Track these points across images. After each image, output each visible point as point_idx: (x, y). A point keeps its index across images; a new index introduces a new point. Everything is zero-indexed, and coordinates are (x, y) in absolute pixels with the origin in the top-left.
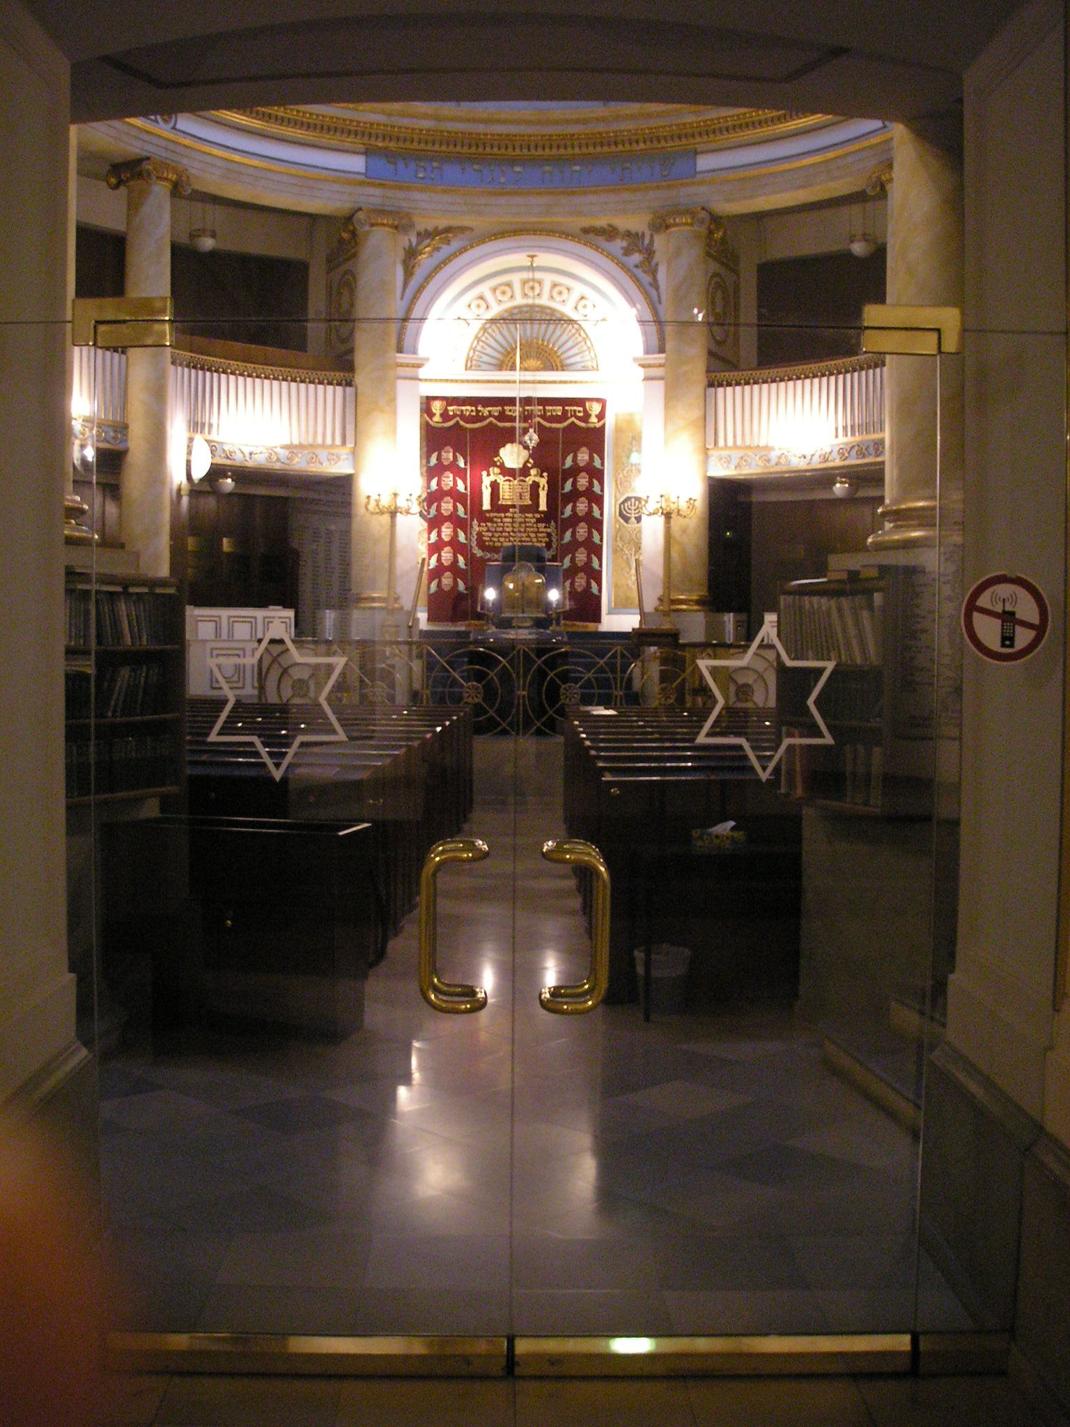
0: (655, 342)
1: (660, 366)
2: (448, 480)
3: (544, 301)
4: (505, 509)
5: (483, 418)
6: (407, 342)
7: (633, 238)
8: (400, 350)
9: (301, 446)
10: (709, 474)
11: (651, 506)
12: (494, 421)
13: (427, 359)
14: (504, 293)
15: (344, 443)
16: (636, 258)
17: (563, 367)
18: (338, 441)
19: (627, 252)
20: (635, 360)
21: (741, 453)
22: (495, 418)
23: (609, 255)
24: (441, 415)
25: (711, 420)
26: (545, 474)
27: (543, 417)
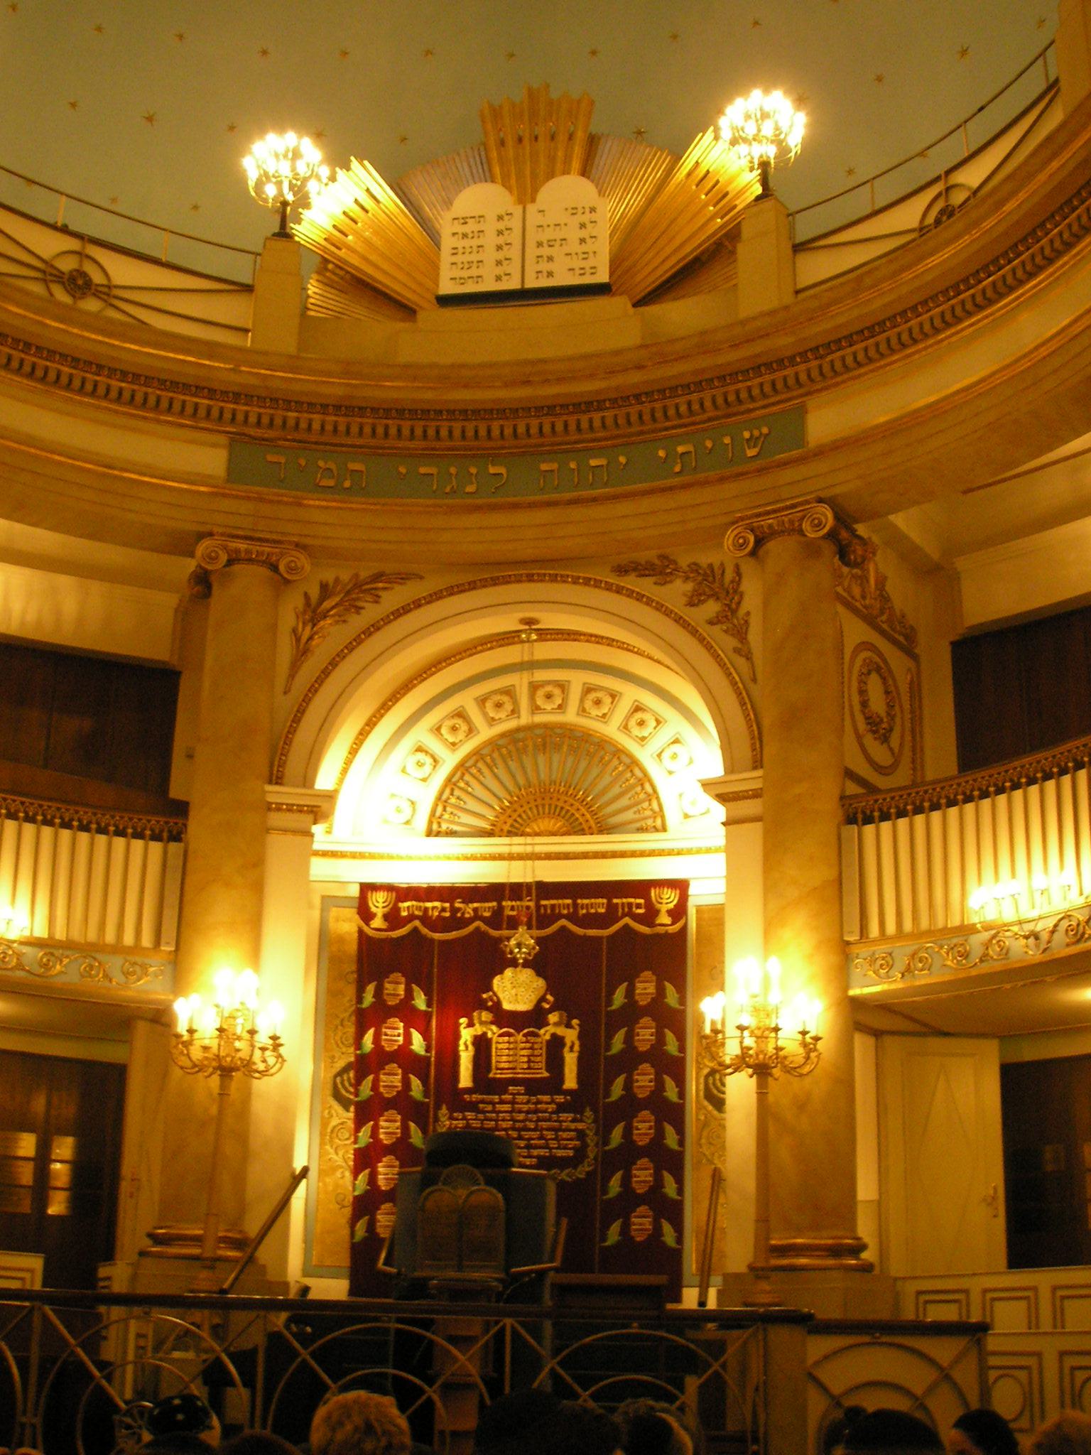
0: (744, 751)
1: (756, 794)
2: (395, 1032)
3: (570, 716)
4: (499, 1086)
5: (464, 923)
6: (294, 765)
8: (276, 778)
9: (69, 945)
10: (853, 992)
11: (731, 1050)
12: (483, 927)
13: (331, 797)
14: (499, 705)
16: (711, 608)
17: (604, 829)
18: (147, 941)
19: (694, 601)
20: (707, 785)
21: (910, 947)
22: (484, 919)
25: (851, 887)
26: (575, 1022)
27: (572, 917)
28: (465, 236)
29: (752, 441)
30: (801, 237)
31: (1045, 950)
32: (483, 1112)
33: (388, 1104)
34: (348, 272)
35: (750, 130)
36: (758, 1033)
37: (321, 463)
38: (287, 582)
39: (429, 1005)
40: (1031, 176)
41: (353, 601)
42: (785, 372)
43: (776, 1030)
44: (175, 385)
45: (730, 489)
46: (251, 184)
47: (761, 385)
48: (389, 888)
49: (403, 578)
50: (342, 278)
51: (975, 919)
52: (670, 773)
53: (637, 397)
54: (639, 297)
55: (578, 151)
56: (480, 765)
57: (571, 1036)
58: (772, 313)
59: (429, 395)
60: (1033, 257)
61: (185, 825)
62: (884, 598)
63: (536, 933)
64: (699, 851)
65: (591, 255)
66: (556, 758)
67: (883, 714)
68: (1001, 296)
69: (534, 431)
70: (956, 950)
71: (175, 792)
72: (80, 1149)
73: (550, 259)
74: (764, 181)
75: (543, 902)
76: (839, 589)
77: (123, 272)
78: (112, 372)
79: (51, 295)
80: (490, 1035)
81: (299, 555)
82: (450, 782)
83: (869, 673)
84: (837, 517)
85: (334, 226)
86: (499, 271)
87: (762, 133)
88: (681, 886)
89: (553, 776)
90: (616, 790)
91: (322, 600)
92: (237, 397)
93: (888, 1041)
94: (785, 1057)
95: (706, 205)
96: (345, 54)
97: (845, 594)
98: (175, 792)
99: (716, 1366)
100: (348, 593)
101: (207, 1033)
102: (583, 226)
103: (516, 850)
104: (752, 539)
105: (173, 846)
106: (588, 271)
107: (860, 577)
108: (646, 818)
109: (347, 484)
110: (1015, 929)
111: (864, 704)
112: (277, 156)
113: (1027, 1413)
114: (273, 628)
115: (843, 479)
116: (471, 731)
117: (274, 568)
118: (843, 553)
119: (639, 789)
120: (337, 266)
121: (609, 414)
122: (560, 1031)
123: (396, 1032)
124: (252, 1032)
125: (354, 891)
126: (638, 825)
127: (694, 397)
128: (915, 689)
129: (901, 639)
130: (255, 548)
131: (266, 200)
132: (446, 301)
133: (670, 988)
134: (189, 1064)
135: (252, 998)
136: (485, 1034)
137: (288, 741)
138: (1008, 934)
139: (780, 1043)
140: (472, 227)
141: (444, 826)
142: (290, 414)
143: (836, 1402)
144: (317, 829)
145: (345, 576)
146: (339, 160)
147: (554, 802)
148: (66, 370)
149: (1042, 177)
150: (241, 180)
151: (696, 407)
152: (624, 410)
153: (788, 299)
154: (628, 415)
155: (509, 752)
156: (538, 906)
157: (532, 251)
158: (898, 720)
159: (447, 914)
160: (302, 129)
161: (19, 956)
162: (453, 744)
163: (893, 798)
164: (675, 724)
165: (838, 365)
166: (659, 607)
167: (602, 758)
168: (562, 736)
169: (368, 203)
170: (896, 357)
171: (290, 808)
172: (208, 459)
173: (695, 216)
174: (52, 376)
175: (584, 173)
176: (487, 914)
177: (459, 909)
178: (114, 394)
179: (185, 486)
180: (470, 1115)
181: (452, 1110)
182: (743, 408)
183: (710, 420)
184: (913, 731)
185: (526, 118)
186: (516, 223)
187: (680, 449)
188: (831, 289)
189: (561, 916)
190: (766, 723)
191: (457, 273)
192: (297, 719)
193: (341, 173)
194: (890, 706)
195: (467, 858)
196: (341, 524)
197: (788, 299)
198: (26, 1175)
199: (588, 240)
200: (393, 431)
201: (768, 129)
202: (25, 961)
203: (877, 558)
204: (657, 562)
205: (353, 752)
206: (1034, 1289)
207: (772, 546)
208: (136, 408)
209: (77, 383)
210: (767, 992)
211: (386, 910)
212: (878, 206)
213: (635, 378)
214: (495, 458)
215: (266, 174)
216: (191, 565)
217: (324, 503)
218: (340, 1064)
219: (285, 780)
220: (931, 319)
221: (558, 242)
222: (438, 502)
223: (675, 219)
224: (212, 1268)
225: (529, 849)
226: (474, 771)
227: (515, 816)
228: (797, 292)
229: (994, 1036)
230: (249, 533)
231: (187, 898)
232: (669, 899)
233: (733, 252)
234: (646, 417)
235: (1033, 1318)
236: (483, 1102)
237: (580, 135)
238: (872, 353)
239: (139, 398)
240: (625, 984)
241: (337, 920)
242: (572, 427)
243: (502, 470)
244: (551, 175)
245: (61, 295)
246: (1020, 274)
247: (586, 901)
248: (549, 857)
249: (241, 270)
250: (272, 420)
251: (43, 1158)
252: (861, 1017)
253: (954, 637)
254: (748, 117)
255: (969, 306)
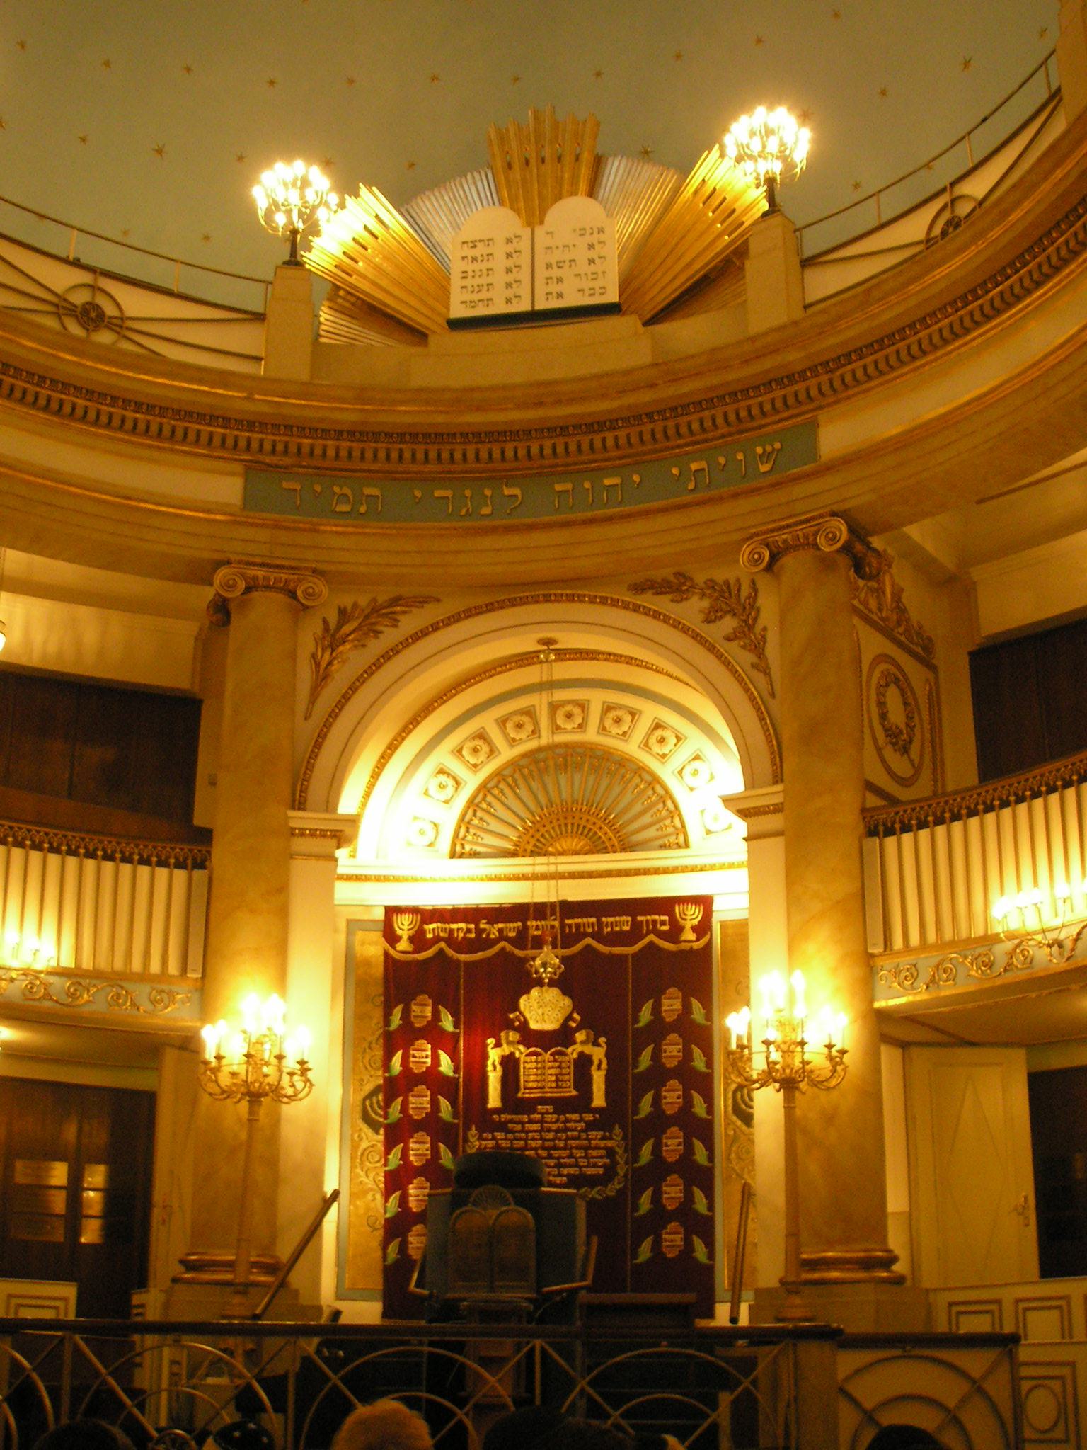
0: (764, 765)
1: (777, 809)
2: (423, 1054)
3: (591, 735)
4: (528, 1106)
5: (489, 943)
9: (97, 975)
10: (878, 1004)
11: (758, 1065)
12: (509, 947)
13: (353, 821)
14: (519, 726)
15: (184, 969)
16: (729, 624)
17: (627, 847)
18: (173, 969)
19: (711, 617)
20: (728, 801)
24: (411, 939)
26: (602, 1040)
27: (598, 936)
28: (474, 259)
29: (765, 456)
30: (807, 253)
31: (1069, 958)
32: (512, 1132)
33: (418, 1126)
34: (358, 298)
35: (756, 146)
36: (784, 1047)
37: (336, 489)
38: (306, 608)
39: (456, 1026)
40: (1034, 186)
41: (374, 623)
42: (796, 387)
43: (802, 1044)
44: (189, 415)
45: (744, 505)
46: (261, 213)
47: (773, 401)
48: (414, 910)
49: (422, 601)
50: (353, 304)
51: (998, 929)
52: (692, 789)
53: (650, 415)
54: (649, 316)
55: (585, 172)
56: (502, 786)
57: (598, 1054)
58: (782, 328)
59: (440, 419)
60: (1040, 265)
61: (209, 853)
62: (900, 609)
63: (561, 952)
64: (722, 867)
65: (601, 275)
66: (577, 778)
67: (903, 726)
68: (1010, 306)
69: (548, 451)
70: (980, 960)
71: (199, 820)
72: (112, 1177)
73: (560, 280)
74: (771, 197)
75: (568, 921)
76: (855, 602)
77: (134, 303)
78: (126, 403)
79: (65, 328)
80: (517, 1055)
81: (315, 580)
82: (472, 803)
83: (887, 685)
84: (851, 530)
85: (344, 253)
86: (510, 293)
87: (767, 150)
88: (704, 902)
89: (575, 795)
90: (638, 808)
91: (340, 625)
92: (251, 426)
93: (915, 1052)
94: (812, 1071)
95: (714, 222)
96: (351, 81)
97: (861, 607)
98: (199, 820)
99: (746, 1383)
100: (367, 617)
101: (235, 1059)
102: (591, 246)
103: (540, 869)
104: (767, 554)
105: (198, 874)
106: (598, 291)
107: (877, 590)
108: (670, 835)
109: (363, 509)
110: (1039, 937)
111: (883, 716)
112: (285, 185)
113: (1061, 1426)
114: (293, 656)
115: (857, 492)
116: (492, 752)
117: (293, 594)
118: (858, 566)
119: (661, 806)
120: (349, 293)
121: (622, 434)
122: (588, 1049)
123: (424, 1054)
124: (280, 1058)
125: (380, 914)
126: (661, 842)
127: (707, 414)
128: (934, 702)
129: (919, 650)
130: (273, 575)
131: (276, 229)
132: (457, 325)
133: (696, 1004)
134: (217, 1090)
135: (280, 1023)
136: (512, 1054)
137: (310, 767)
138: (1031, 943)
139: (806, 1057)
140: (480, 250)
141: (468, 848)
142: (305, 441)
143: (869, 1417)
144: (341, 854)
145: (363, 601)
146: (347, 186)
147: (576, 821)
148: (81, 402)
149: (1046, 186)
150: (251, 208)
151: (708, 424)
152: (638, 429)
153: (798, 314)
154: (641, 434)
155: (531, 773)
156: (563, 926)
157: (541, 273)
158: (917, 730)
159: (473, 935)
160: (309, 158)
161: (46, 986)
162: (475, 766)
163: (913, 810)
164: (696, 740)
165: (848, 378)
166: (677, 625)
167: (623, 776)
168: (583, 755)
169: (377, 229)
170: (905, 369)
171: (313, 833)
172: (221, 487)
173: (702, 234)
174: (67, 409)
175: (592, 193)
176: (512, 934)
177: (484, 930)
178: (129, 425)
179: (201, 515)
180: (499, 1135)
181: (481, 1131)
182: (755, 424)
183: (723, 436)
184: (932, 742)
185: (533, 140)
186: (525, 245)
187: (694, 466)
188: (841, 302)
189: (585, 935)
190: (786, 735)
191: (468, 297)
192: (318, 745)
193: (349, 200)
194: (909, 717)
195: (490, 879)
196: (359, 549)
197: (798, 314)
198: (59, 1203)
199: (597, 261)
200: (407, 455)
201: (773, 145)
202: (52, 990)
203: (894, 570)
204: (672, 578)
205: (376, 775)
206: (1066, 1298)
207: (788, 561)
208: (151, 438)
209: (92, 415)
210: (793, 1006)
211: (411, 933)
212: (885, 218)
213: (646, 397)
214: (509, 480)
215: (275, 204)
216: (209, 593)
217: (340, 529)
218: (368, 1088)
219: (308, 804)
220: (940, 330)
221: (568, 263)
222: (455, 524)
223: (684, 237)
224: (245, 1293)
225: (552, 869)
226: (496, 792)
227: (538, 835)
228: (806, 307)
229: (1020, 1045)
230: (267, 561)
231: (212, 926)
232: (693, 915)
233: (741, 268)
234: (659, 436)
235: (1066, 1328)
236: (511, 1121)
237: (586, 157)
238: (882, 365)
239: (154, 428)
240: (651, 1002)
241: (363, 943)
242: (585, 447)
243: (517, 491)
244: (558, 197)
245: (75, 329)
246: (1027, 282)
247: (610, 919)
248: (572, 876)
249: (252, 299)
250: (286, 447)
251: (75, 1187)
252: (887, 1029)
253: (971, 648)
254: (752, 134)
255: (977, 316)
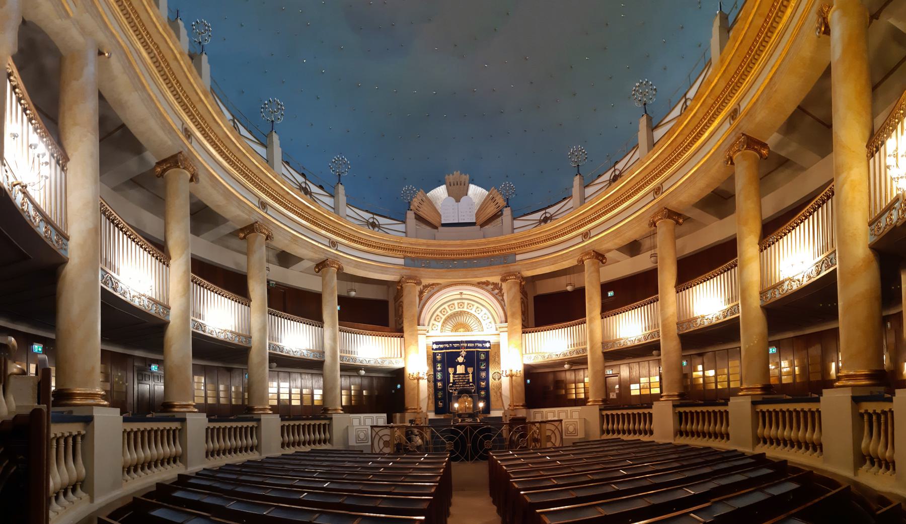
6: (421, 322)
7: (495, 285)
16: (497, 291)
19: (493, 290)
23: (488, 291)
190: (509, 314)
